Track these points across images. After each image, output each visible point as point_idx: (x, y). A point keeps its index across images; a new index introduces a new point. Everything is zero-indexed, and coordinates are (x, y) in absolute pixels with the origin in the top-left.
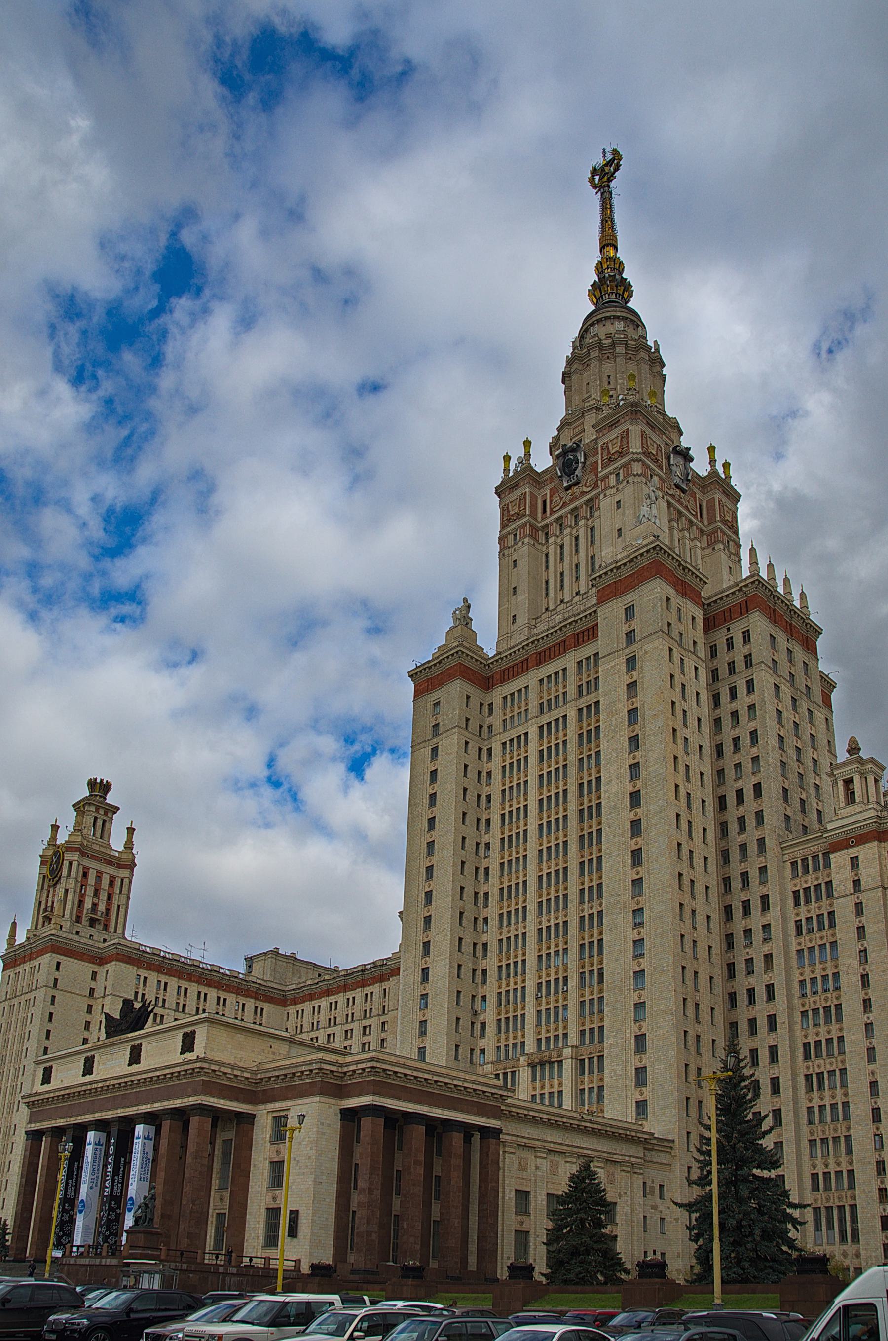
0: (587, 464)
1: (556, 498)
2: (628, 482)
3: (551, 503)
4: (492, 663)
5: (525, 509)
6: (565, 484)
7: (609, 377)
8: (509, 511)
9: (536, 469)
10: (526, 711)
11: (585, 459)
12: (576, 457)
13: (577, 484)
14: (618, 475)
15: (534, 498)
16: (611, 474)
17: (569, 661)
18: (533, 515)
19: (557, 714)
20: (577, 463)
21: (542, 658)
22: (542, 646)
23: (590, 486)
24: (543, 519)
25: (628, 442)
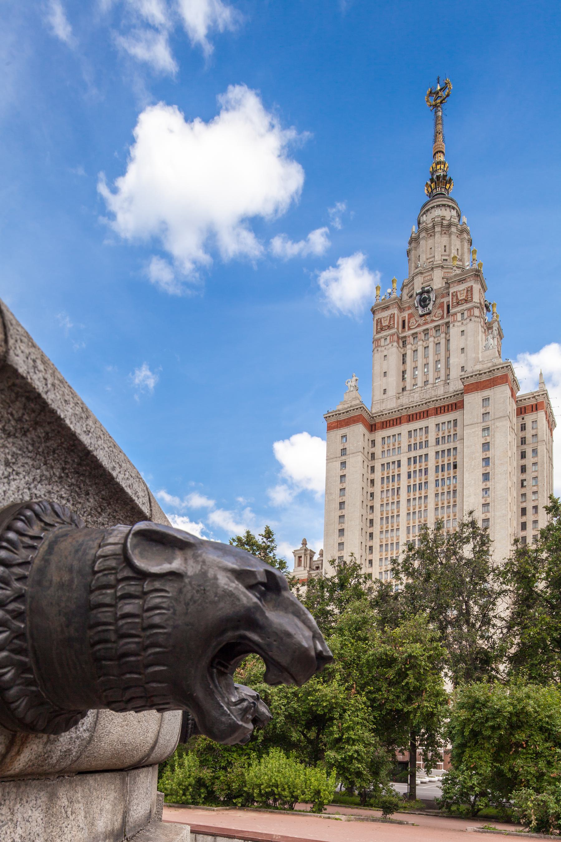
0: (436, 302)
1: (413, 320)
2: (470, 320)
3: (409, 322)
4: (376, 417)
5: (394, 324)
6: (420, 313)
7: (445, 246)
8: (381, 323)
10: (399, 448)
12: (429, 297)
13: (429, 314)
14: (463, 314)
16: (459, 312)
17: (431, 422)
18: (398, 328)
19: (423, 452)
20: (430, 300)
21: (411, 418)
22: (411, 412)
24: (402, 332)
25: (472, 294)
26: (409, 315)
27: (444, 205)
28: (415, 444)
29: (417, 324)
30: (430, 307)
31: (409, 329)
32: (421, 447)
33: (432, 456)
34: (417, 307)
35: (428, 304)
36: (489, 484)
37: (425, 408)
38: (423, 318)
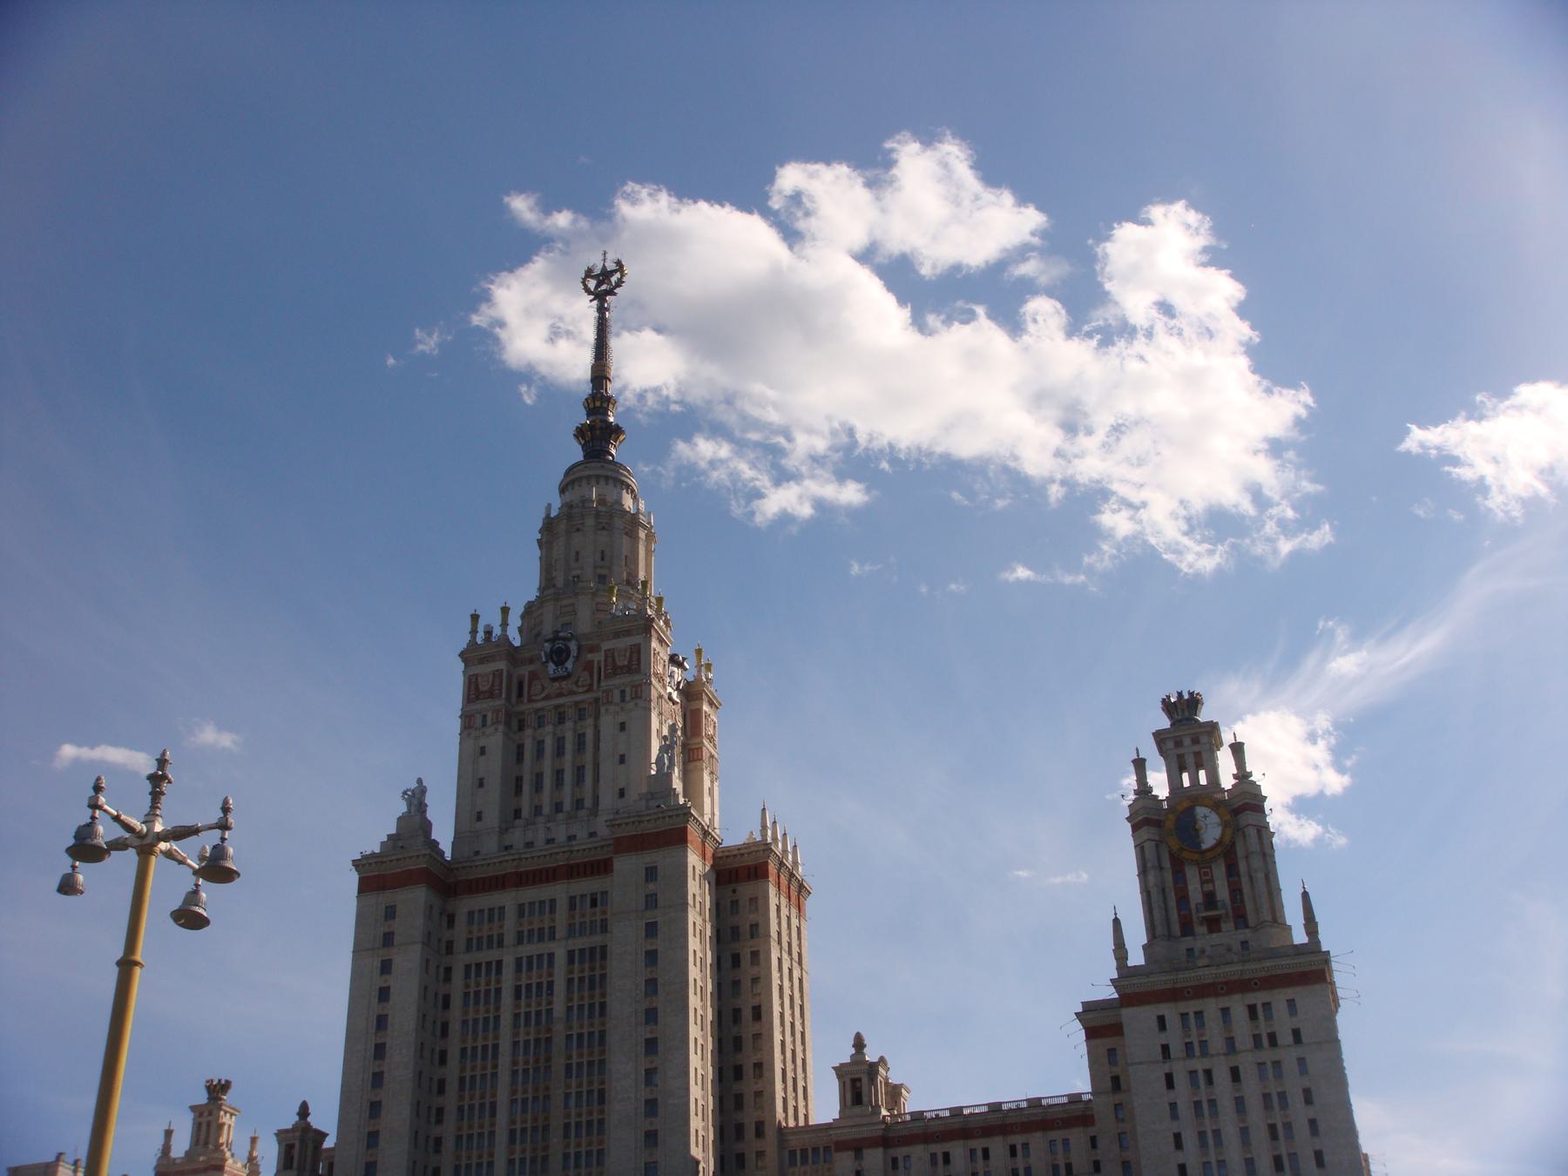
1: (537, 687)
3: (529, 687)
4: (457, 869)
5: (501, 690)
9: (513, 643)
11: (579, 652)
15: (510, 676)
17: (559, 892)
18: (508, 698)
23: (583, 686)
28: (531, 932)
29: (543, 695)
30: (569, 665)
31: (530, 701)
34: (547, 662)
38: (556, 684)
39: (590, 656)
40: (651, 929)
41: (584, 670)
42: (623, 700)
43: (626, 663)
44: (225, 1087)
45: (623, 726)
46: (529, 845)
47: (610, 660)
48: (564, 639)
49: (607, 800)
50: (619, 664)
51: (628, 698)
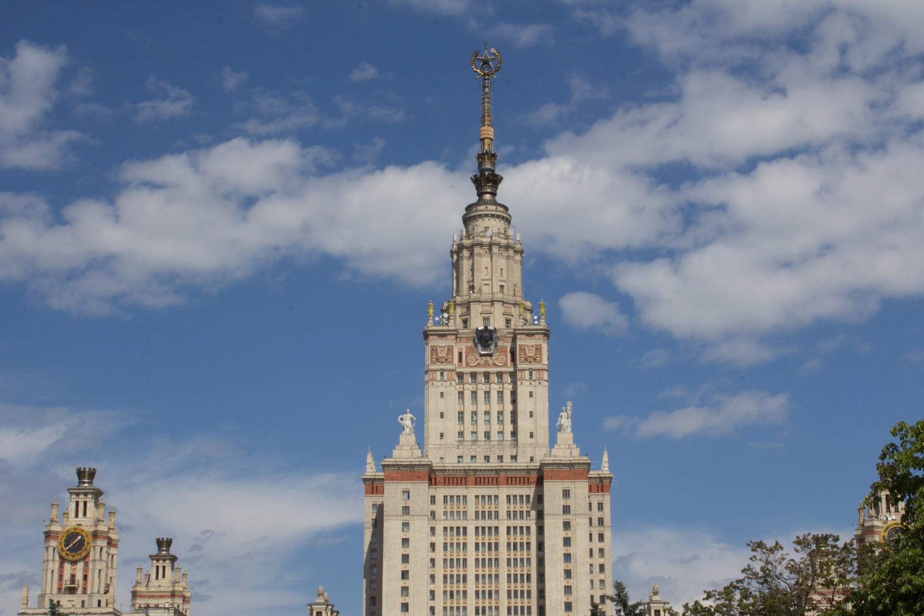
3: (466, 359)
4: (437, 470)
5: (452, 358)
7: (502, 269)
13: (490, 355)
17: (503, 492)
21: (479, 482)
26: (467, 348)
27: (498, 216)
28: (483, 512)
29: (476, 363)
30: (492, 347)
31: (467, 365)
32: (490, 517)
33: (503, 530)
35: (490, 344)
36: (571, 582)
37: (493, 474)
39: (505, 344)
40: (567, 525)
41: (501, 352)
42: (531, 378)
43: (532, 355)
44: (169, 543)
45: (531, 395)
46: (473, 457)
47: (522, 353)
48: (491, 331)
49: (523, 436)
50: (530, 355)
51: (534, 378)
